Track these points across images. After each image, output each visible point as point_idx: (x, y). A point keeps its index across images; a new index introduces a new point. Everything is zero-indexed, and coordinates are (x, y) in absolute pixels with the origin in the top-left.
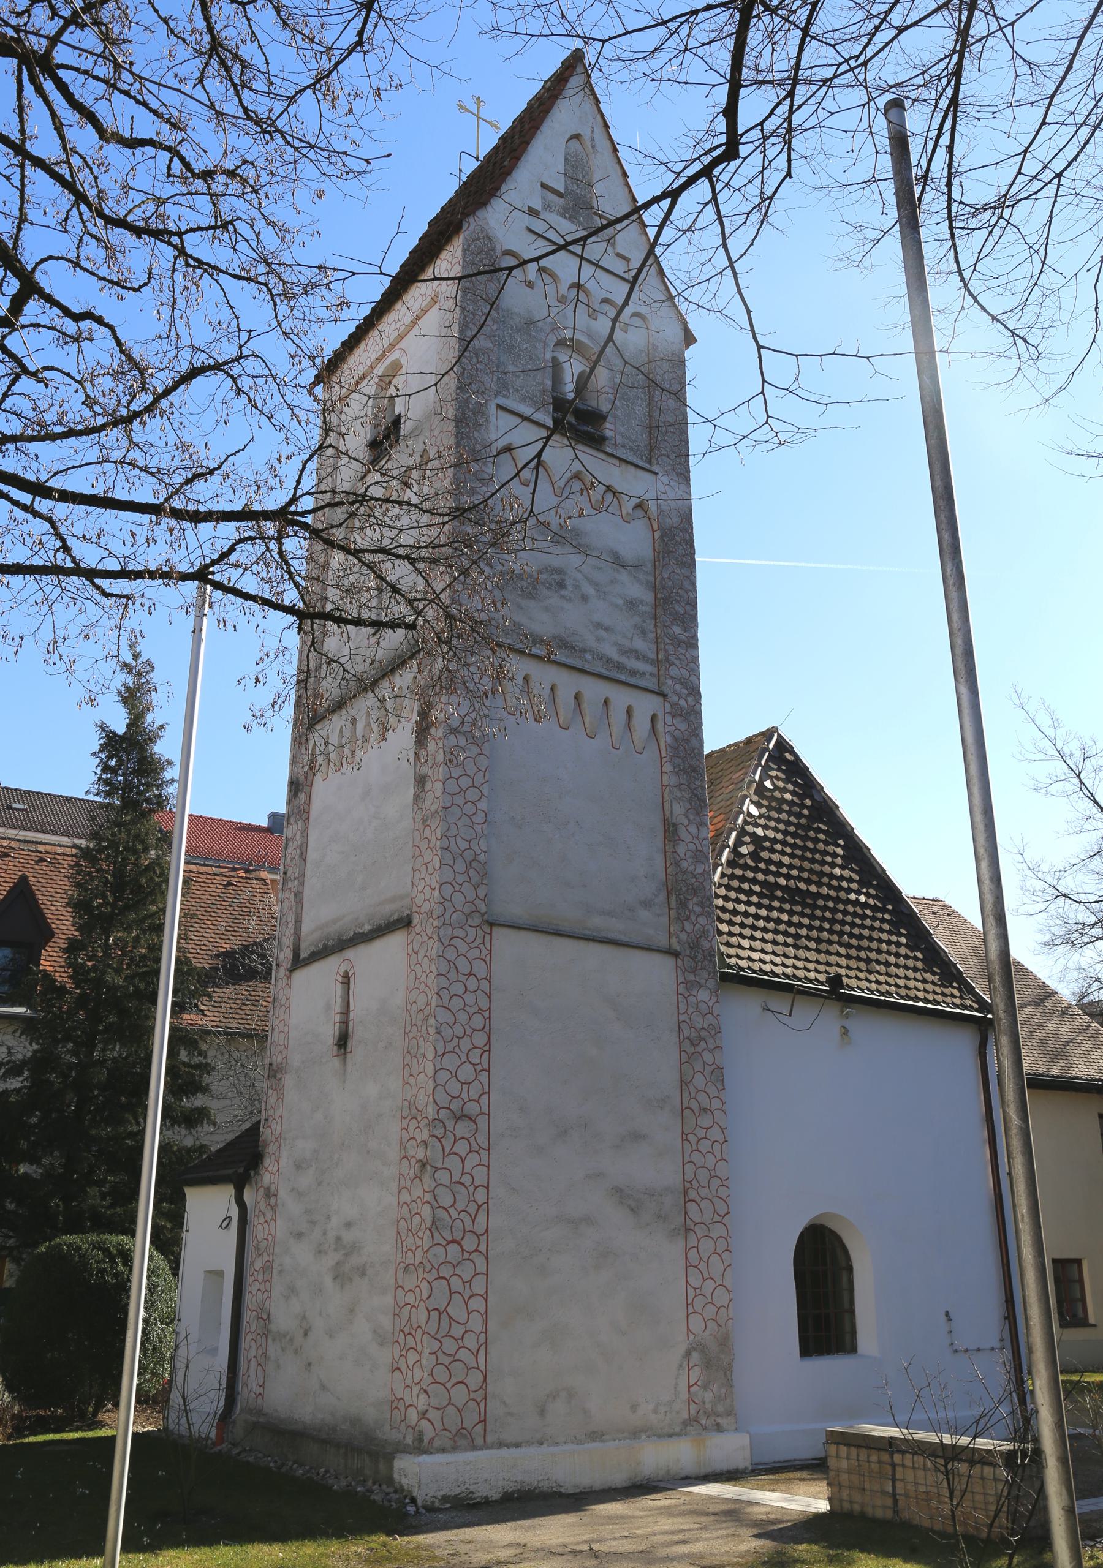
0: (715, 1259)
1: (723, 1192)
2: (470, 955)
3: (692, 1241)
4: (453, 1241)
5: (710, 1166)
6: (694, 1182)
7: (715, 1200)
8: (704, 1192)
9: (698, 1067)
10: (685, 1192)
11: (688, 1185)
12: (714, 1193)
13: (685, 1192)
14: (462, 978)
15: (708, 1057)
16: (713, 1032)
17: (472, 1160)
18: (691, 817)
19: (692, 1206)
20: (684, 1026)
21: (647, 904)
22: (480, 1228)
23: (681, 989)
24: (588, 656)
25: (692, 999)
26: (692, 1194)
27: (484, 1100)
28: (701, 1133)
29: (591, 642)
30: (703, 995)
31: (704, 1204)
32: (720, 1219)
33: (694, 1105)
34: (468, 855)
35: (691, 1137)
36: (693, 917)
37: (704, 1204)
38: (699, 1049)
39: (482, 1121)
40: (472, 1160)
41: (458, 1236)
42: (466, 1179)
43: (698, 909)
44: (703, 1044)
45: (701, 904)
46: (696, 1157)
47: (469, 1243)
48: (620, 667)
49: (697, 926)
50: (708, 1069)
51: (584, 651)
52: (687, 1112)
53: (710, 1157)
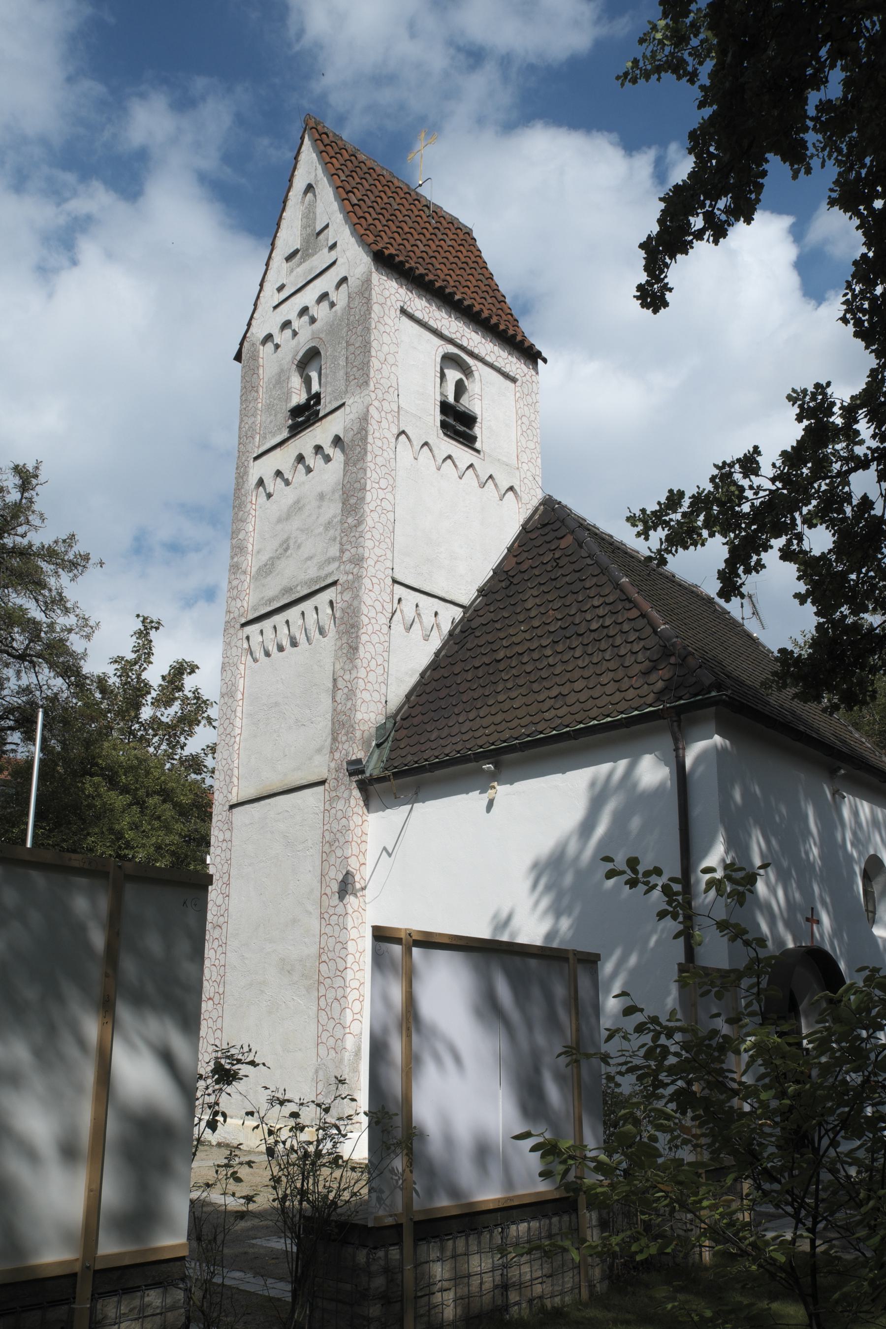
0: (336, 1004)
1: (343, 953)
2: (224, 829)
3: (322, 991)
4: (210, 999)
5: (336, 935)
6: (326, 948)
7: (338, 960)
8: (331, 955)
9: (332, 860)
10: (320, 956)
11: (322, 951)
12: (337, 954)
13: (320, 956)
14: (220, 844)
15: (339, 853)
16: (344, 832)
17: (220, 950)
18: (346, 667)
19: (323, 967)
20: (327, 834)
21: (319, 751)
22: (221, 991)
23: (328, 807)
24: (299, 588)
25: (333, 811)
26: (324, 958)
27: (226, 915)
28: (331, 911)
29: (303, 577)
30: (340, 805)
31: (331, 963)
32: (339, 973)
33: (328, 891)
34: (225, 769)
35: (326, 916)
36: (340, 747)
37: (331, 963)
38: (333, 848)
39: (224, 927)
40: (220, 950)
41: (212, 995)
42: (217, 963)
43: (344, 738)
44: (337, 844)
45: (347, 734)
46: (328, 930)
47: (216, 1000)
48: (318, 579)
49: (344, 751)
50: (339, 860)
51: (297, 585)
52: (324, 897)
53: (337, 927)
